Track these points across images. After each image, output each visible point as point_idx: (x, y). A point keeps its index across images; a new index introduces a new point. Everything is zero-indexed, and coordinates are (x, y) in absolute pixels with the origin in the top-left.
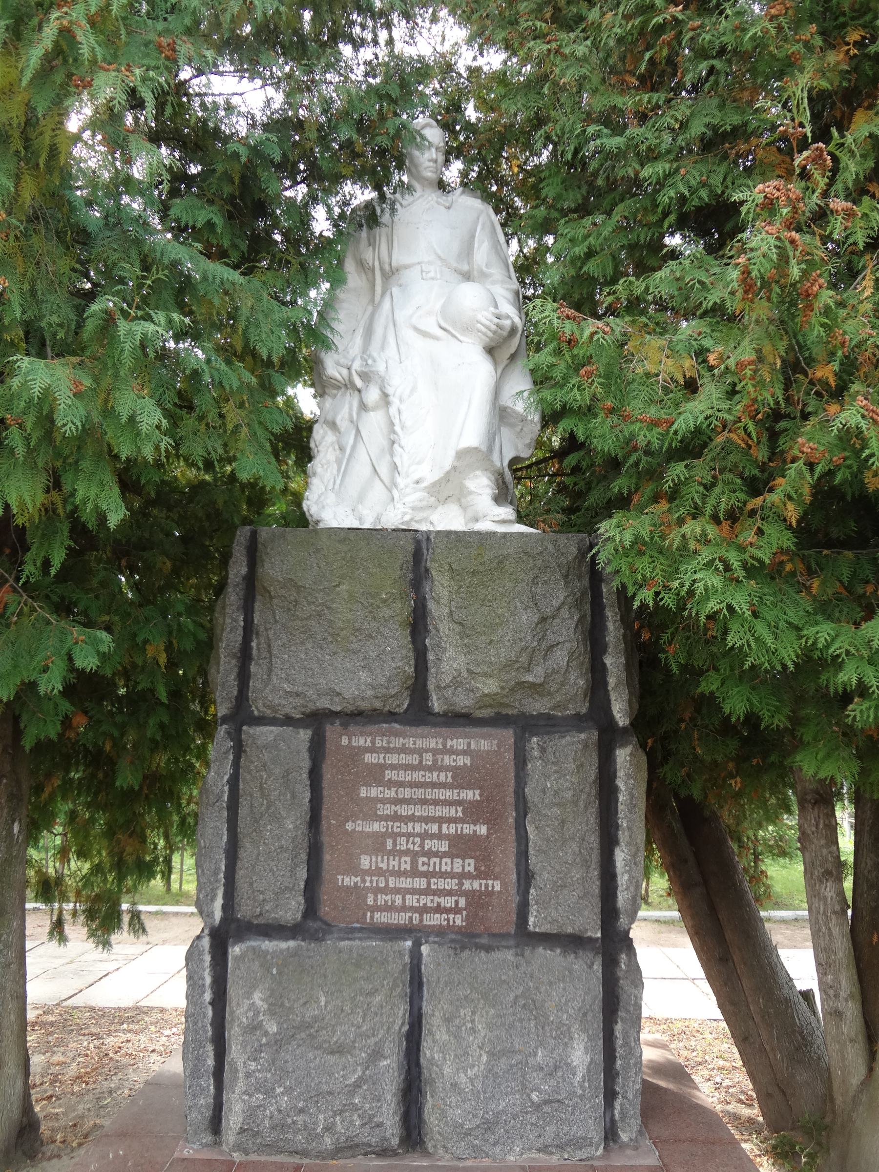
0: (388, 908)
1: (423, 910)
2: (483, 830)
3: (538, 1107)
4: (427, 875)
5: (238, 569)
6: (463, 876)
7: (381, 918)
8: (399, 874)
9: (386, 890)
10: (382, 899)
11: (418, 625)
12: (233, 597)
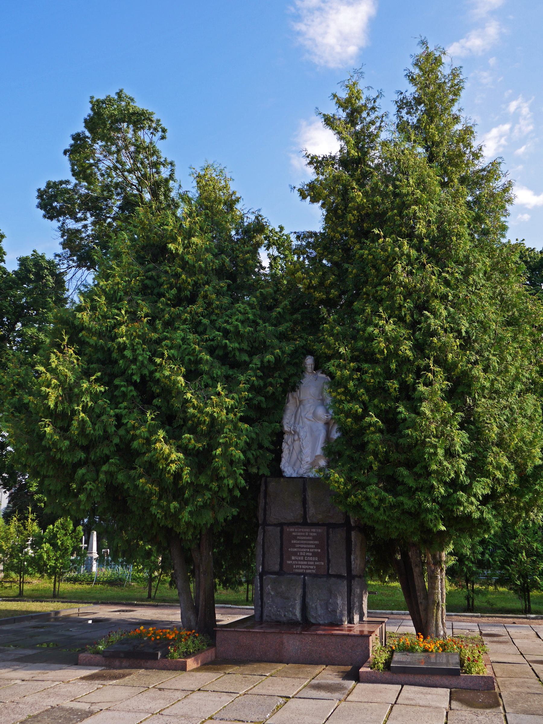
0: (298, 568)
1: (306, 569)
2: (319, 550)
4: (307, 561)
5: (263, 488)
6: (315, 561)
7: (297, 571)
8: (301, 561)
9: (298, 564)
10: (297, 566)
11: (304, 502)
12: (262, 495)
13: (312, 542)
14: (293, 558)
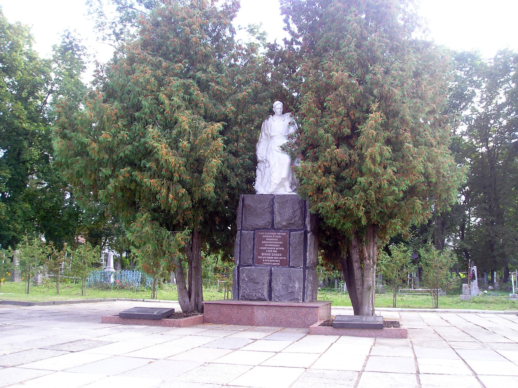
3: (290, 293)
8: (268, 256)
9: (266, 259)
11: (272, 213)
13: (276, 242)
14: (263, 254)
